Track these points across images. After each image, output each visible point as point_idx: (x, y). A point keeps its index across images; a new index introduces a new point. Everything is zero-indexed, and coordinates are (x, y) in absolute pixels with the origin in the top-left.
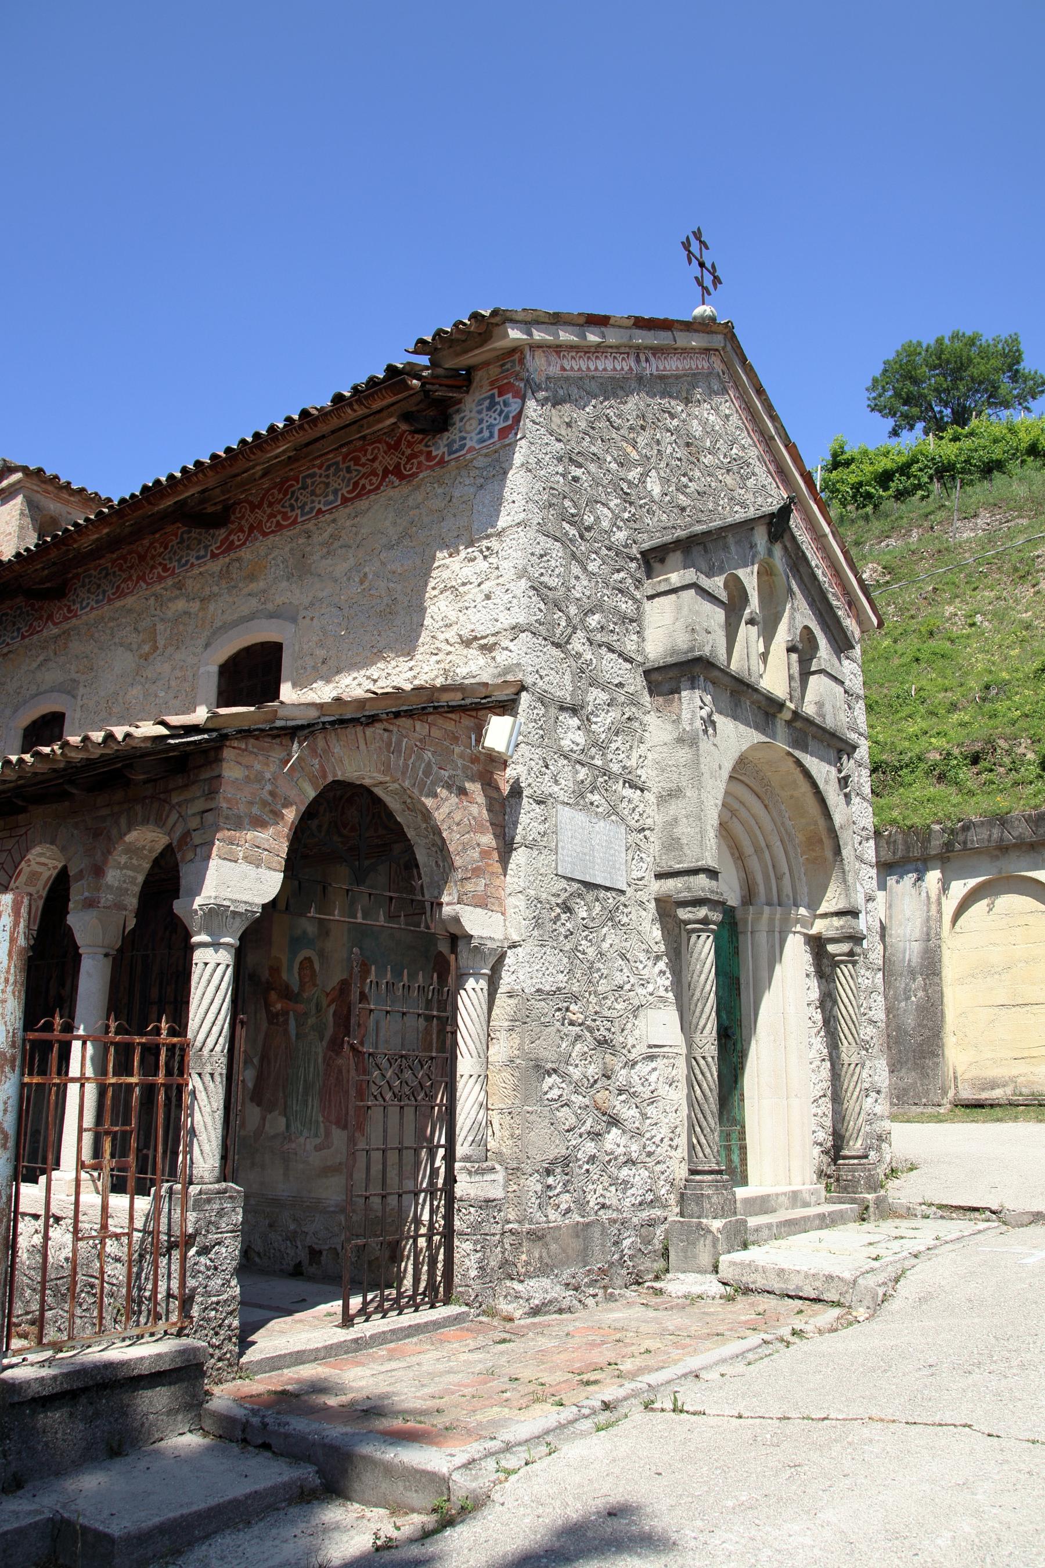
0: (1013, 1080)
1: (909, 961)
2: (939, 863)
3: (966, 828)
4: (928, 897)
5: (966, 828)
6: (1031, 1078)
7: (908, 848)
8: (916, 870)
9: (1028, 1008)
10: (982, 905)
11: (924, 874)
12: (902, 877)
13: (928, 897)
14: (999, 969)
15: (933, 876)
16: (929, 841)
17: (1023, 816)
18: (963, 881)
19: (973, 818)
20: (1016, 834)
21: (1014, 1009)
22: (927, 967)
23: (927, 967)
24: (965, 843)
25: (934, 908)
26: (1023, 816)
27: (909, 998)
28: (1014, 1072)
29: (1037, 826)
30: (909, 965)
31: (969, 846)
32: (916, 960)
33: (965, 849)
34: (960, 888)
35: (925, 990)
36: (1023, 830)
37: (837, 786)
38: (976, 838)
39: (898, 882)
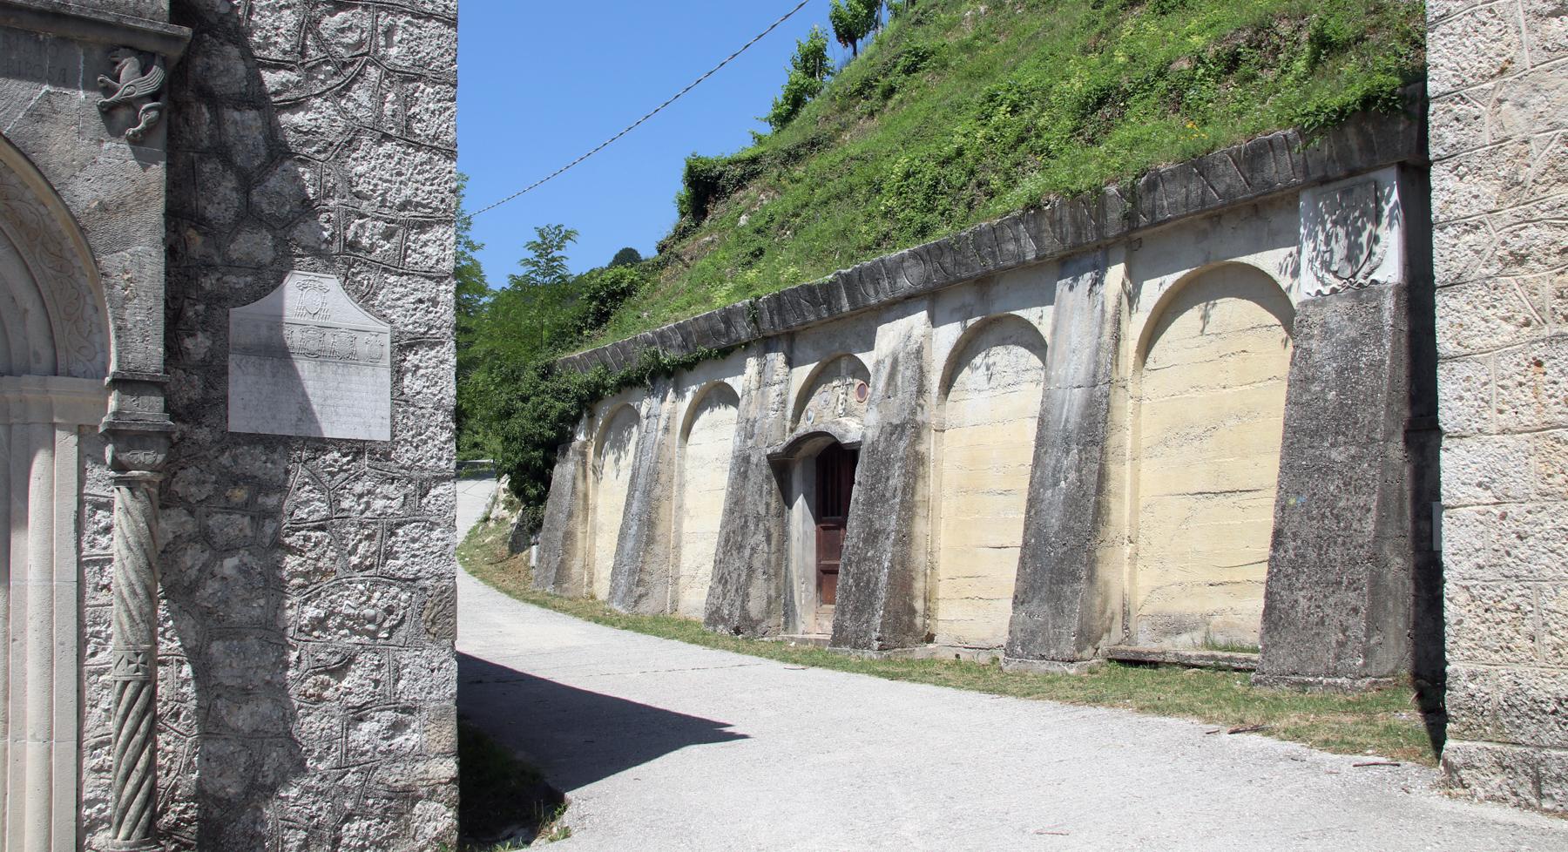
0: (1206, 619)
1: (1067, 421)
2: (1123, 251)
3: (1152, 186)
4: (1103, 311)
5: (1152, 186)
6: (1232, 618)
7: (1079, 228)
8: (1094, 267)
9: (1235, 498)
10: (1190, 318)
11: (1103, 275)
12: (1076, 280)
13: (1103, 311)
14: (1199, 431)
15: (1116, 274)
16: (1105, 216)
17: (1230, 154)
18: (1158, 280)
19: (1163, 167)
20: (1221, 188)
21: (1217, 499)
22: (1086, 431)
23: (1086, 431)
24: (1153, 213)
25: (1108, 329)
26: (1230, 154)
27: (1056, 484)
28: (1209, 607)
29: (1252, 170)
30: (1065, 430)
31: (1159, 217)
32: (1075, 419)
33: (1155, 223)
34: (1153, 290)
35: (1079, 470)
36: (1230, 179)
37: (96, 123)
38: (1169, 200)
39: (1071, 288)
